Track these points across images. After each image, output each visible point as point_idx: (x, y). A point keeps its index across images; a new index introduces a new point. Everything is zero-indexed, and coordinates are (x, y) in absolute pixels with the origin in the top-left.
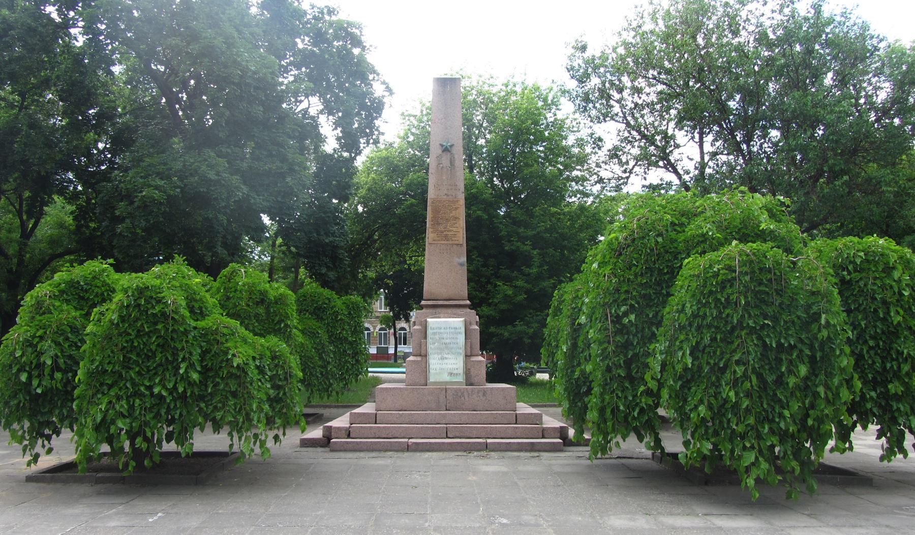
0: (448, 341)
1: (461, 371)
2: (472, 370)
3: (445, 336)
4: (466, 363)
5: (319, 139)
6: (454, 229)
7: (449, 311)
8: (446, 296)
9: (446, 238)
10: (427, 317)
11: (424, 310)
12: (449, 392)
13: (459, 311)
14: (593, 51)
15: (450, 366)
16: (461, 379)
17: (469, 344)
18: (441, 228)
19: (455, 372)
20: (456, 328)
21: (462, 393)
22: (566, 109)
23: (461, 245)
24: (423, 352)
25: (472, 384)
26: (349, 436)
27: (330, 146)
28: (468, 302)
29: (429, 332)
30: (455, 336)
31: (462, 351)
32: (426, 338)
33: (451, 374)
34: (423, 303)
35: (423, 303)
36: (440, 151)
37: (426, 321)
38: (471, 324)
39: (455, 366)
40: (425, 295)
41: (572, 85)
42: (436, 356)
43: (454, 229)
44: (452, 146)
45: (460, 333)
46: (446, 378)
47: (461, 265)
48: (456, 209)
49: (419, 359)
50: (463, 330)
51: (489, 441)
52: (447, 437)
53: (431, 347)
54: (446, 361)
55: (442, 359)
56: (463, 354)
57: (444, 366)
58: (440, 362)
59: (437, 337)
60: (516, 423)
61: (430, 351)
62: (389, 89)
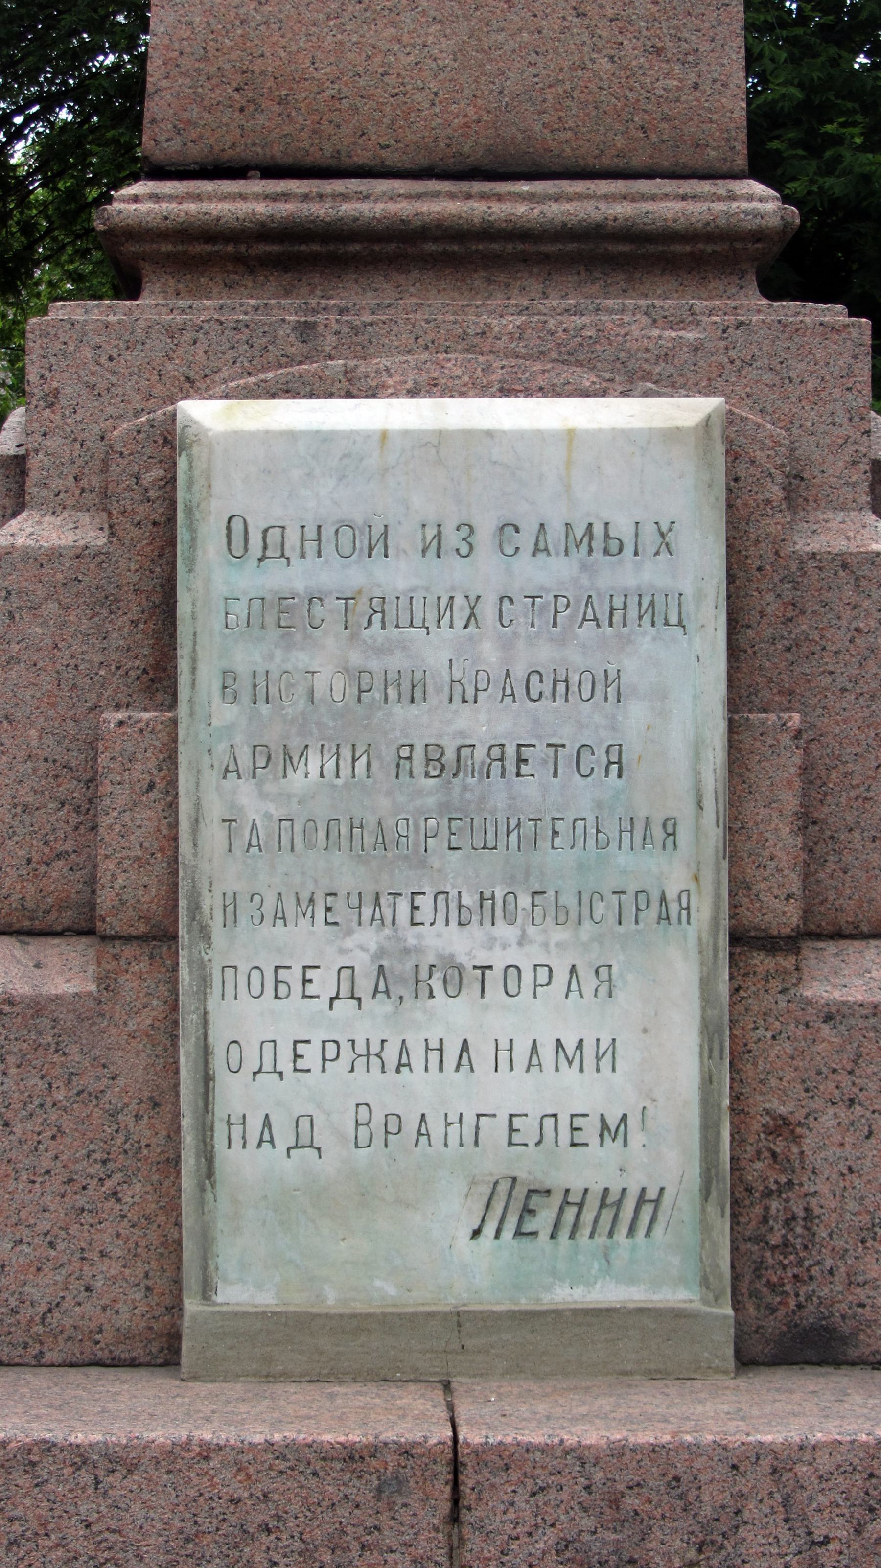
0: (484, 724)
1: (669, 1157)
3: (435, 651)
4: (736, 1047)
7: (503, 312)
8: (449, 117)
10: (193, 386)
11: (152, 305)
16: (667, 1270)
19: (592, 1169)
20: (595, 541)
24: (122, 890)
28: (758, 202)
29: (214, 584)
30: (581, 651)
32: (159, 678)
33: (520, 1205)
35: (137, 202)
37: (168, 440)
38: (798, 491)
39: (582, 1092)
42: (304, 940)
45: (656, 611)
50: (698, 567)
53: (240, 806)
54: (451, 1016)
55: (401, 979)
56: (706, 911)
57: (423, 1091)
58: (369, 1022)
59: (323, 662)
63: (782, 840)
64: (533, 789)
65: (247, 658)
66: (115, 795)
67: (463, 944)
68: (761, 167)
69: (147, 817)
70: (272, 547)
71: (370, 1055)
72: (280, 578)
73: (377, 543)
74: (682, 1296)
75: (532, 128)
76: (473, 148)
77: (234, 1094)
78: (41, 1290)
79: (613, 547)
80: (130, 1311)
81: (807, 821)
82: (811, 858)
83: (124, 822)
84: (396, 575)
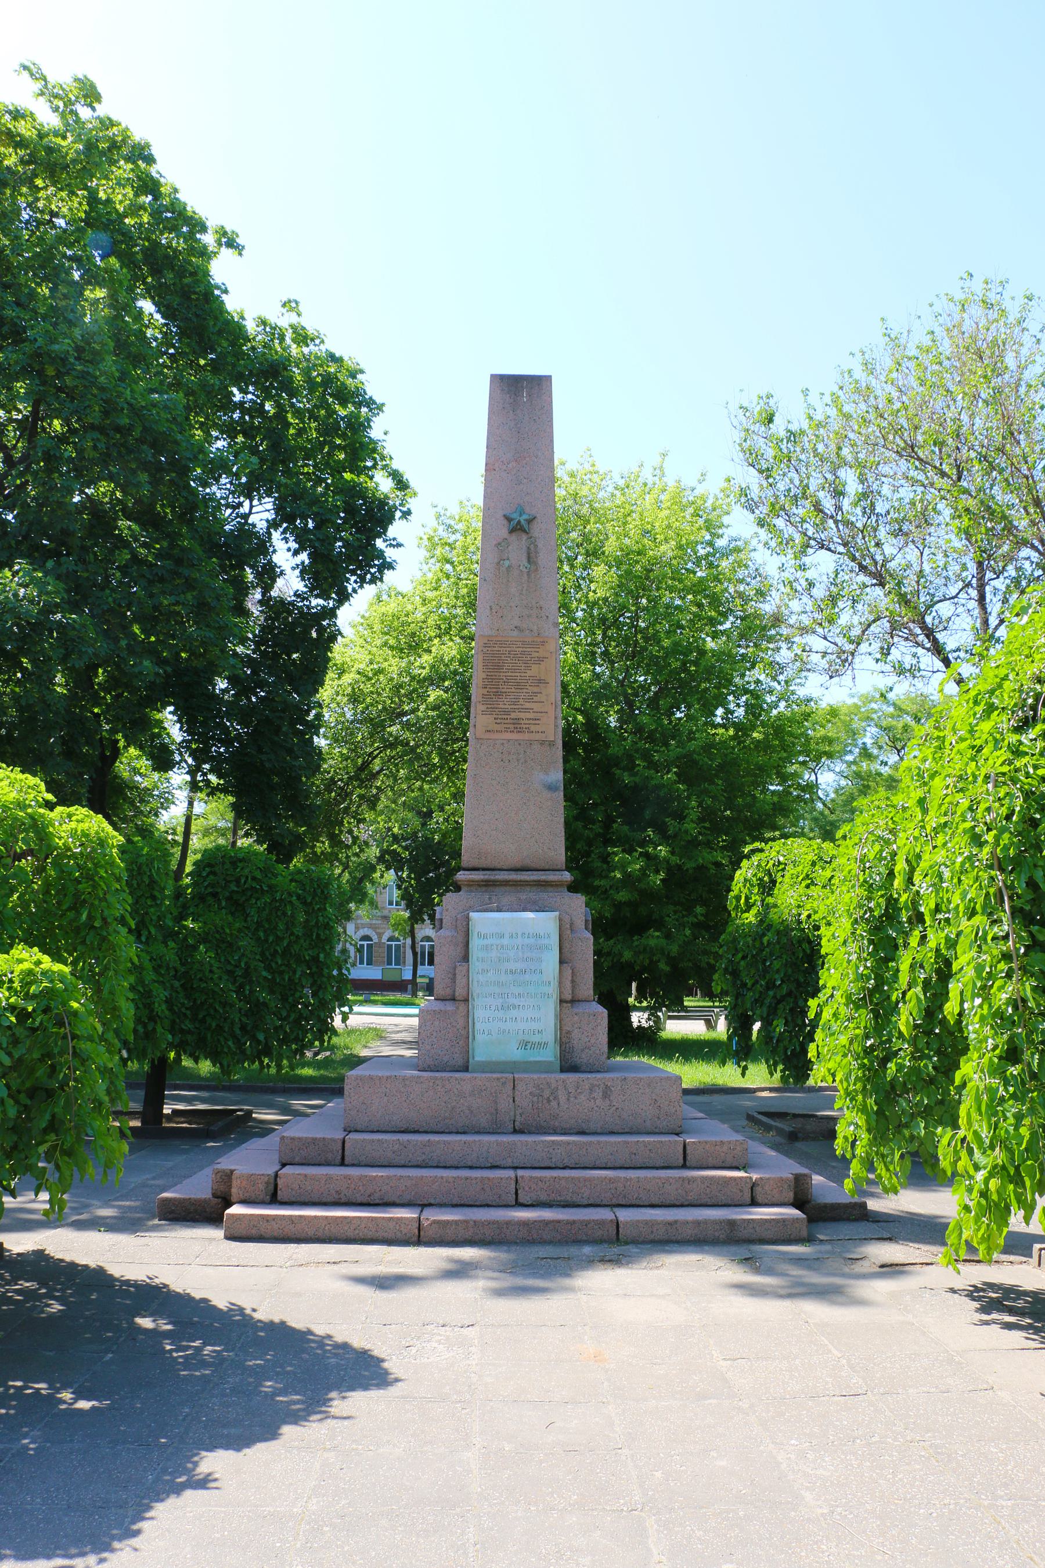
0: (519, 966)
2: (576, 1034)
3: (512, 954)
4: (560, 1019)
5: (269, 574)
6: (536, 707)
8: (514, 861)
9: (517, 726)
12: (520, 1087)
13: (544, 896)
14: (791, 415)
15: (522, 1026)
17: (568, 973)
18: (504, 704)
19: (536, 1038)
20: (537, 936)
21: (554, 1092)
22: (739, 525)
23: (552, 744)
24: (459, 993)
25: (574, 1069)
26: (274, 1199)
27: (290, 584)
28: (567, 876)
29: (475, 943)
31: (553, 990)
32: (466, 958)
33: (525, 1044)
34: (461, 876)
36: (504, 532)
37: (468, 919)
39: (535, 1026)
40: (466, 859)
41: (752, 479)
43: (536, 707)
44: (530, 521)
46: (513, 1053)
47: (551, 788)
48: (540, 660)
49: (450, 1007)
51: (625, 1215)
52: (519, 1204)
54: (513, 1013)
56: (555, 996)
58: (500, 1014)
59: (494, 954)
60: (684, 1166)
61: (475, 989)
62: (402, 485)
63: (568, 984)
64: (527, 977)
65: (481, 954)
66: (458, 977)
67: (516, 1002)
68: (568, 869)
69: (464, 980)
70: (485, 937)
71: (501, 1020)
72: (486, 942)
73: (502, 936)
74: (552, 1059)
75: (528, 862)
76: (518, 866)
77: (478, 1026)
78: (445, 1059)
79: (540, 937)
80: (460, 1062)
81: (573, 981)
82: (573, 988)
83: (460, 981)
84: (505, 941)
